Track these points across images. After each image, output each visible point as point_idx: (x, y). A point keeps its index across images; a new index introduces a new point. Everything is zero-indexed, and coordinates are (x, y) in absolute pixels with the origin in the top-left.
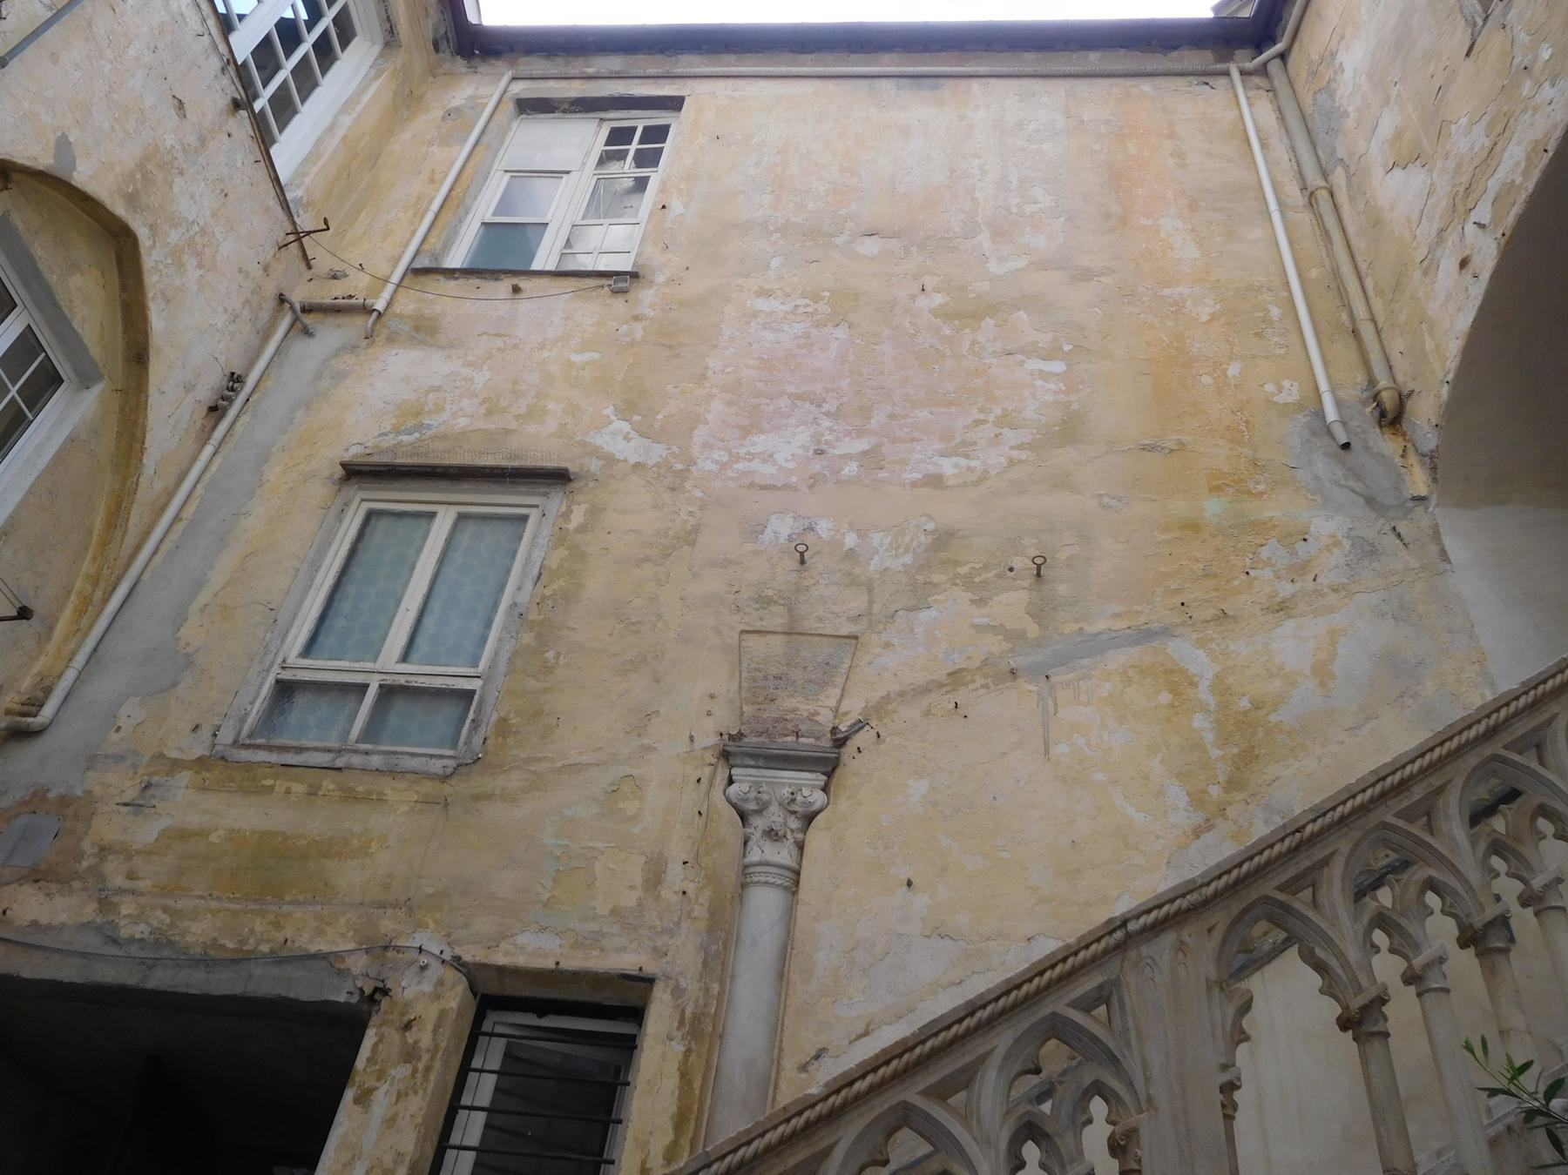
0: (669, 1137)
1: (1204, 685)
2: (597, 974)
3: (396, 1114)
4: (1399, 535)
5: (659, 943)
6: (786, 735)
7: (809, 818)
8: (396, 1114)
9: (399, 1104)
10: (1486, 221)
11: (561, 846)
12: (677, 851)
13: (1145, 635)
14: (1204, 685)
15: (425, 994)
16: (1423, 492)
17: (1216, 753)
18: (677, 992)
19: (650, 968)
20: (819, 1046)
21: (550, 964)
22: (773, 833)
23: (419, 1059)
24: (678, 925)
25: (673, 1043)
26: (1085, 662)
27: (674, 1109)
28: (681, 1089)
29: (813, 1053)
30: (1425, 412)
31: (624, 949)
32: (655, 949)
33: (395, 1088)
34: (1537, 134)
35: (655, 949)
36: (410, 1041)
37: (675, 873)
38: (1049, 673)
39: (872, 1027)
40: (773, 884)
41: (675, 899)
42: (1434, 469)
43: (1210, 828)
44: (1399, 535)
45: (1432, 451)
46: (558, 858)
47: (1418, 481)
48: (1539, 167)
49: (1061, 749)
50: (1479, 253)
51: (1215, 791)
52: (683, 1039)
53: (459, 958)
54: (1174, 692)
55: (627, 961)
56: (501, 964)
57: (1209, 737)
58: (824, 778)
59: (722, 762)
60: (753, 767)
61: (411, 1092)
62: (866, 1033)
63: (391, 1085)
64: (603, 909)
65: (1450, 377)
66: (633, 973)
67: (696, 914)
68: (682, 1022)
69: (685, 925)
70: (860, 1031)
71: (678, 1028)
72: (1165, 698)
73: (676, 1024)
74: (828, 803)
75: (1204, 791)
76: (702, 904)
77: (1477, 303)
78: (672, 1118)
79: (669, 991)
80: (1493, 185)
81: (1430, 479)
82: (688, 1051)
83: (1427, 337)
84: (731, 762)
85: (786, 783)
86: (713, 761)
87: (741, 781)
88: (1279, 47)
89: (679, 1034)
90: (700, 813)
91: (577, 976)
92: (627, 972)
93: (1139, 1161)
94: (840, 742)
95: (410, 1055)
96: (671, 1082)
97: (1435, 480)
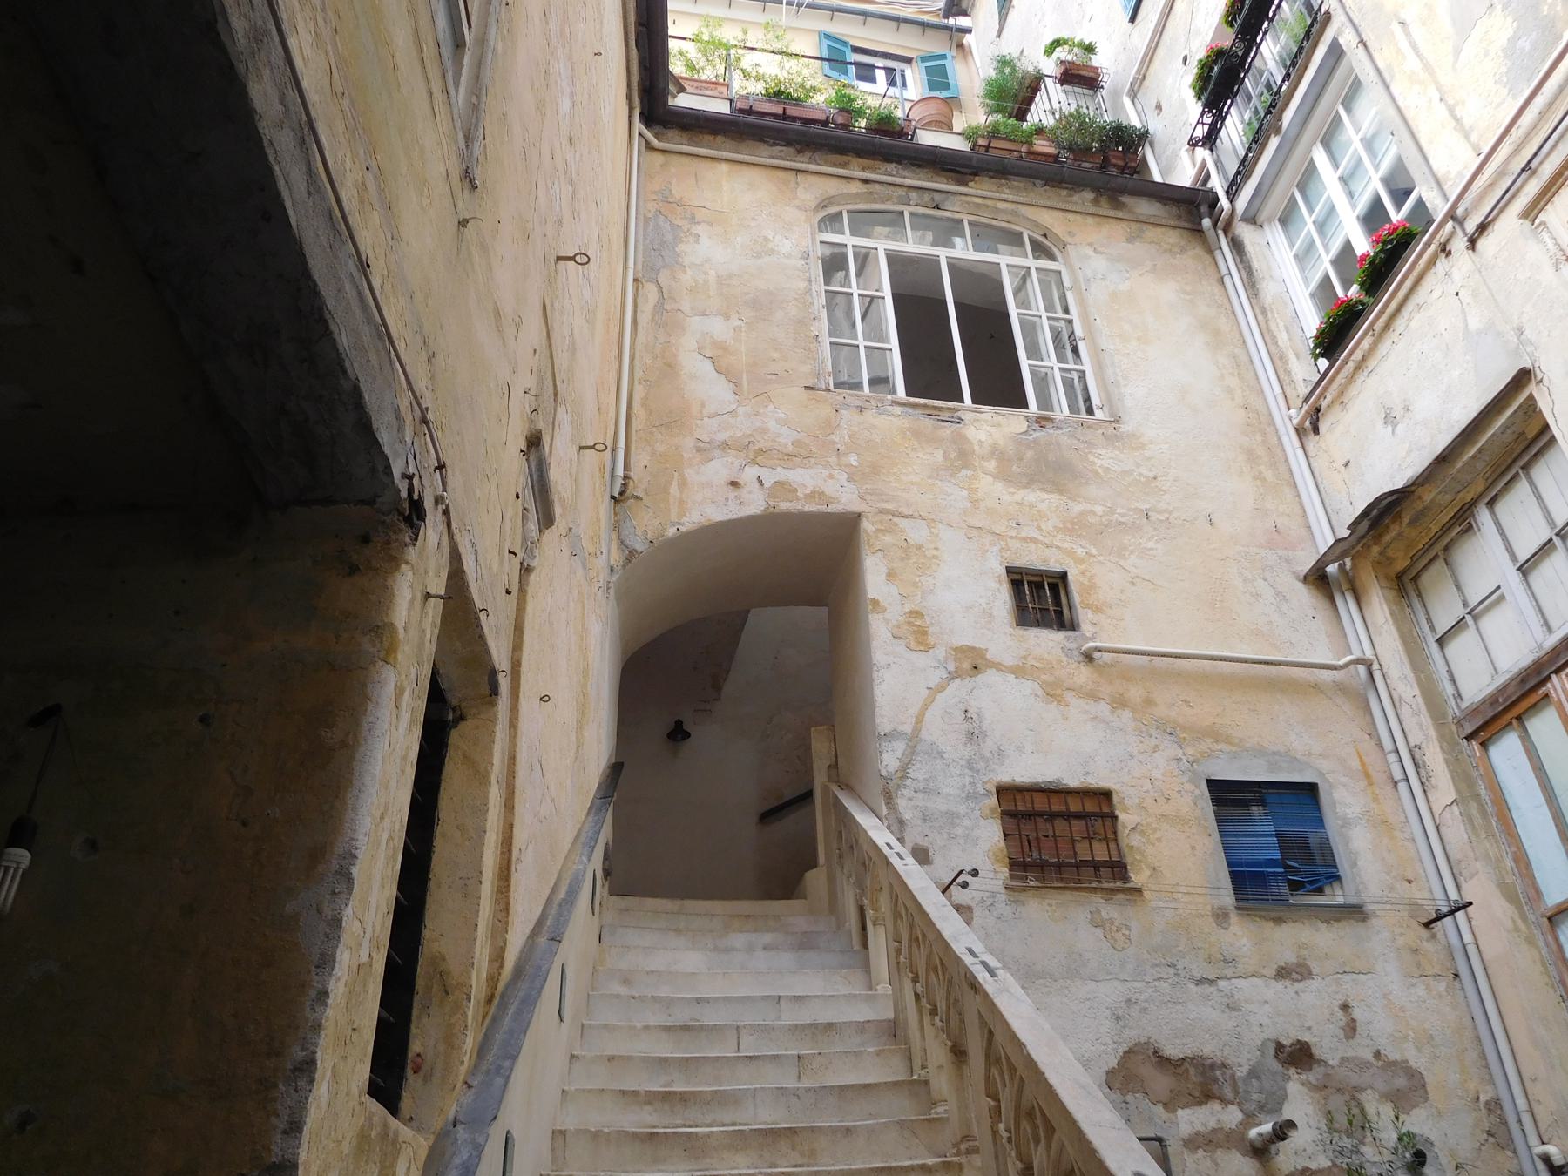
10: (767, 484)
30: (647, 526)
34: (830, 488)
42: (629, 560)
45: (636, 551)
48: (819, 507)
50: (750, 492)
65: (683, 529)
77: (730, 517)
80: (781, 474)
83: (675, 483)
88: (655, 142)
97: (624, 567)
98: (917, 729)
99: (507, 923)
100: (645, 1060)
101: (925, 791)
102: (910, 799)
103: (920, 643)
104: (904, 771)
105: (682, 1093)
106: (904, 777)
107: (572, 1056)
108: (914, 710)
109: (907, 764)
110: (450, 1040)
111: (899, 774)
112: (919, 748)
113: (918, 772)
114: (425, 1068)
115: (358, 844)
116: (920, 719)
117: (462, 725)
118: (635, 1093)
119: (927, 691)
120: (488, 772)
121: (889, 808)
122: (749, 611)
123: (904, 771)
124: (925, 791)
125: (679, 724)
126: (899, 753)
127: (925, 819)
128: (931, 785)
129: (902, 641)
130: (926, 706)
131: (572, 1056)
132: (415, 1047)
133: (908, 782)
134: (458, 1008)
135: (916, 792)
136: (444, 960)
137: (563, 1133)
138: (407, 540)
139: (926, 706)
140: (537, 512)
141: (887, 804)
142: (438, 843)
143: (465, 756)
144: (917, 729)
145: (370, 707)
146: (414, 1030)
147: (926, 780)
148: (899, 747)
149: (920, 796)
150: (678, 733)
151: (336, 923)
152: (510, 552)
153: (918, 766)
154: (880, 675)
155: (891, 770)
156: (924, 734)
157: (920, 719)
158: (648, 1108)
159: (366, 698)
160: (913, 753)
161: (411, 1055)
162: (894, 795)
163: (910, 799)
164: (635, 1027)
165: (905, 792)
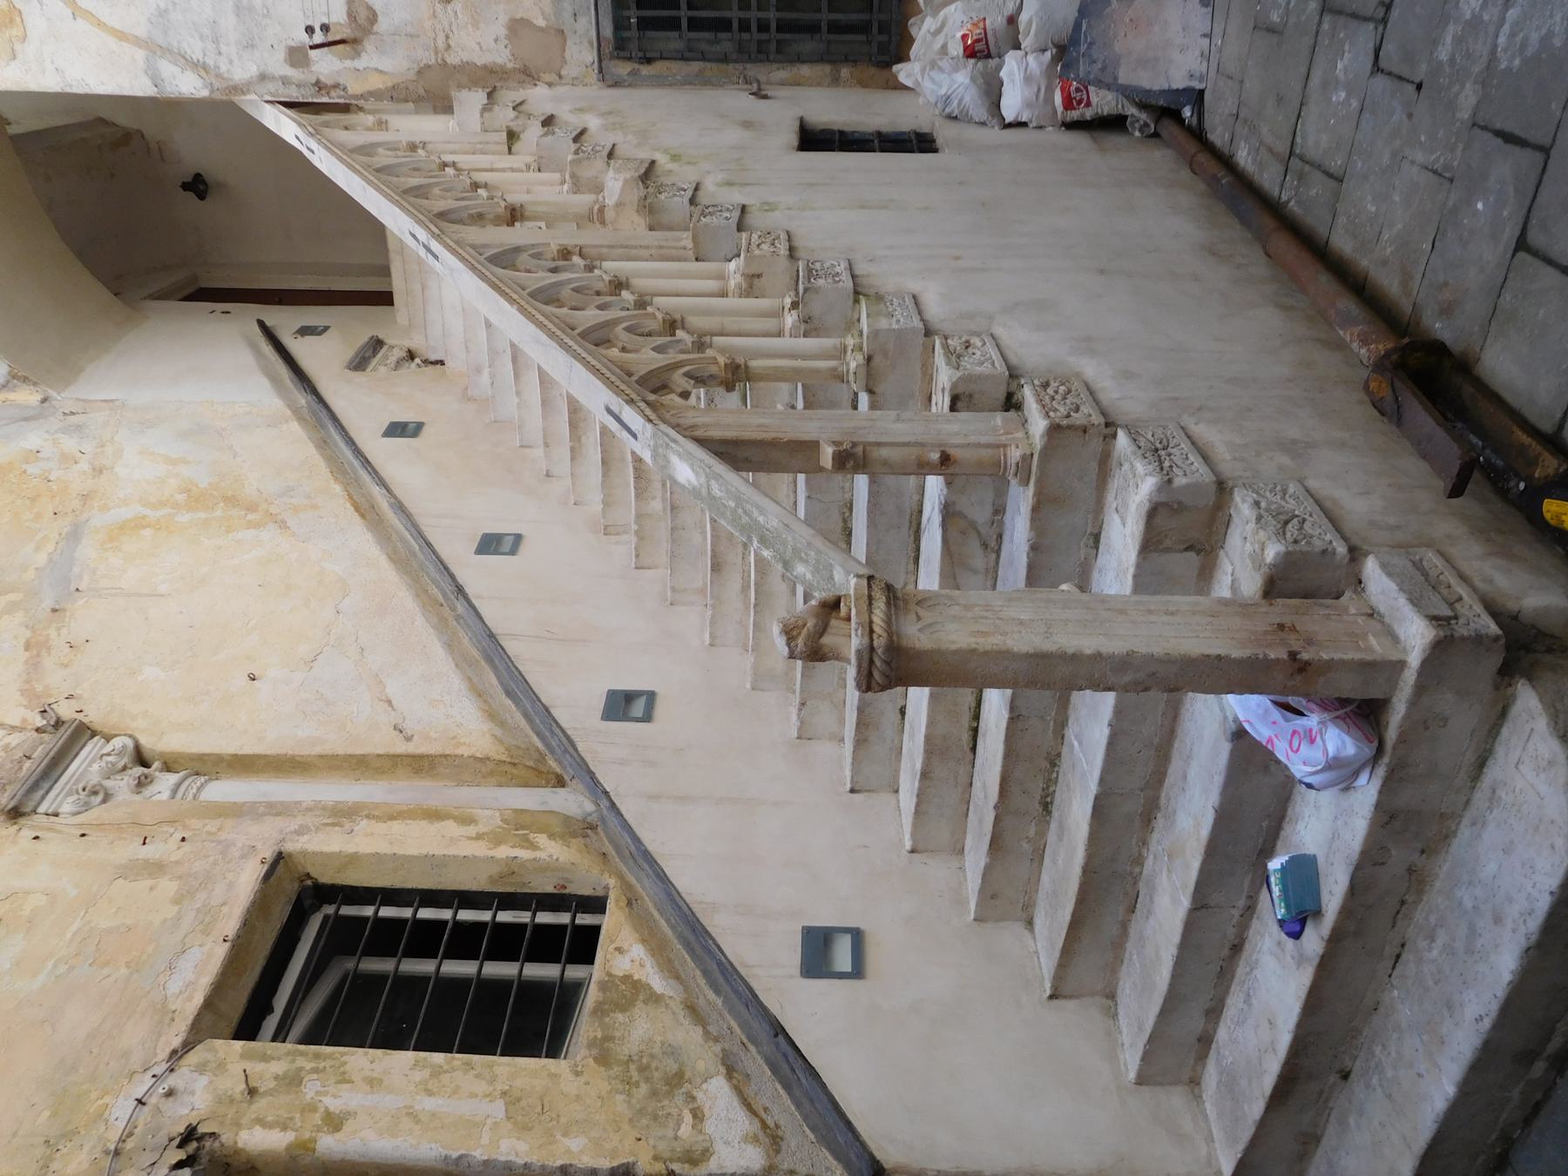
0: (450, 824)
1: (147, 512)
2: (253, 903)
3: (365, 1079)
4: (72, 413)
5: (237, 855)
6: (21, 768)
7: (141, 759)
8: (365, 1079)
9: (353, 1078)
11: (55, 966)
12: (131, 850)
13: (75, 535)
14: (147, 512)
15: (211, 1082)
16: (39, 397)
17: (219, 513)
18: (301, 831)
19: (269, 854)
20: (392, 729)
21: (222, 951)
22: (143, 778)
23: (301, 1069)
24: (219, 842)
25: (356, 828)
26: (76, 570)
27: (423, 823)
28: (404, 818)
29: (397, 733)
31: (231, 885)
32: (243, 857)
33: (331, 1089)
35: (243, 857)
36: (273, 1084)
37: (151, 852)
38: (73, 588)
39: (384, 698)
40: (202, 785)
41: (186, 846)
42: (25, 379)
43: (284, 522)
44: (72, 413)
45: (9, 373)
46: (72, 968)
47: (27, 396)
49: (162, 589)
51: (251, 517)
52: (354, 821)
53: (174, 1052)
54: (149, 526)
55: (247, 879)
56: (202, 1000)
57: (202, 515)
58: (96, 738)
59: (22, 821)
60: (47, 792)
61: (342, 1069)
62: (390, 702)
63: (326, 1094)
64: (171, 911)
66: (264, 870)
67: (214, 830)
68: (333, 825)
69: (223, 836)
70: (386, 705)
71: (342, 826)
72: (147, 532)
73: (337, 828)
74: (130, 736)
75: (250, 521)
76: (205, 825)
78: (431, 823)
79: (297, 838)
81: (32, 387)
82: (368, 817)
84: (27, 810)
85: (85, 769)
86: (16, 827)
87: (60, 805)
89: (347, 826)
90: (83, 835)
91: (248, 924)
92: (262, 875)
93: (576, 246)
94: (59, 723)
95: (293, 1081)
96: (397, 827)
97: (35, 384)
98: (137, 42)
99: (456, 756)
100: (544, 417)
101: (216, 41)
102: (231, 62)
103: (12, 21)
104: (199, 67)
105: (570, 413)
106: (205, 67)
107: (548, 475)
108: (113, 43)
109: (186, 60)
110: (543, 868)
111: (203, 73)
112: (161, 41)
113: (195, 49)
114: (562, 883)
115: (438, 1155)
116: (122, 36)
117: (314, 875)
118: (572, 450)
119: (79, 20)
120: (347, 856)
121: (248, 92)
122: (18, 140)
123: (199, 67)
124: (216, 41)
125: (186, 187)
126: (177, 70)
127: (250, 46)
128: (206, 31)
129: (18, 47)
130: (100, 24)
131: (548, 475)
132: (550, 889)
133: (210, 62)
134: (523, 864)
135: (220, 53)
136: (491, 877)
137: (606, 527)
138: (217, 1144)
139: (100, 24)
140: (76, 755)
141: (244, 93)
142: (409, 885)
143: (339, 872)
144: (137, 42)
145: (349, 1158)
146: (539, 891)
147: (202, 38)
148: (167, 69)
149: (224, 48)
150: (198, 186)
151: (486, 1163)
152: (144, 844)
153: (185, 45)
154: (74, 83)
155: (199, 83)
156: (141, 31)
157: (122, 36)
158: (583, 439)
159: (342, 1161)
160: (170, 51)
161: (556, 891)
162: (231, 83)
163: (231, 62)
164: (518, 404)
165: (223, 68)
